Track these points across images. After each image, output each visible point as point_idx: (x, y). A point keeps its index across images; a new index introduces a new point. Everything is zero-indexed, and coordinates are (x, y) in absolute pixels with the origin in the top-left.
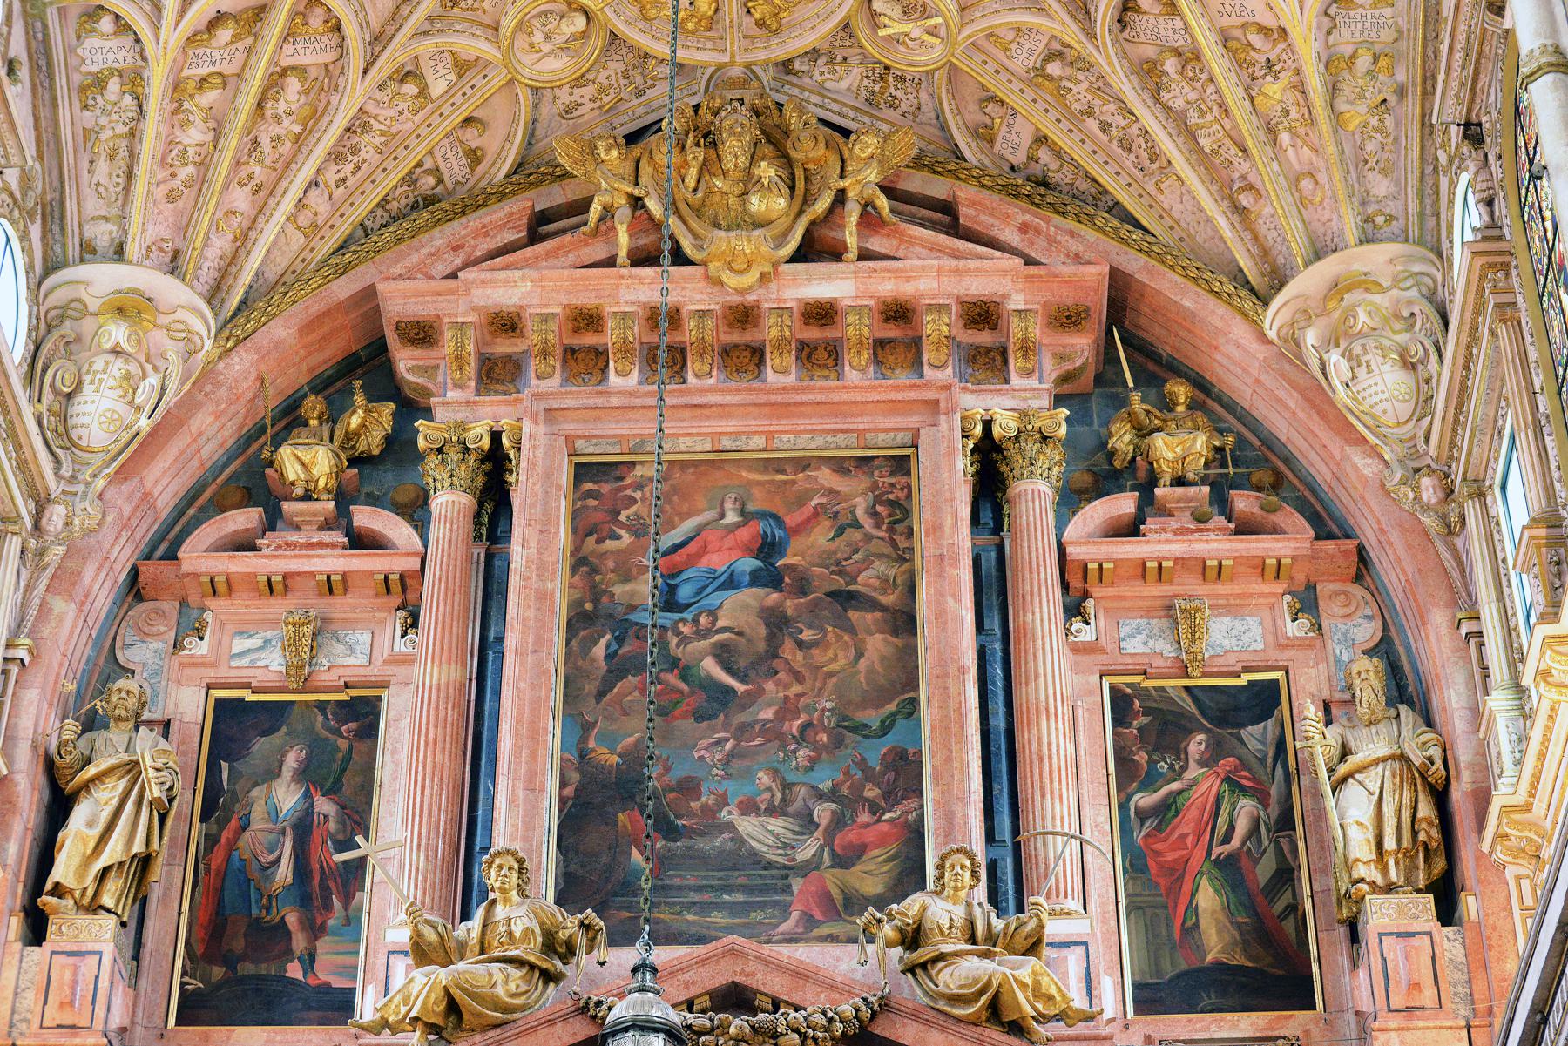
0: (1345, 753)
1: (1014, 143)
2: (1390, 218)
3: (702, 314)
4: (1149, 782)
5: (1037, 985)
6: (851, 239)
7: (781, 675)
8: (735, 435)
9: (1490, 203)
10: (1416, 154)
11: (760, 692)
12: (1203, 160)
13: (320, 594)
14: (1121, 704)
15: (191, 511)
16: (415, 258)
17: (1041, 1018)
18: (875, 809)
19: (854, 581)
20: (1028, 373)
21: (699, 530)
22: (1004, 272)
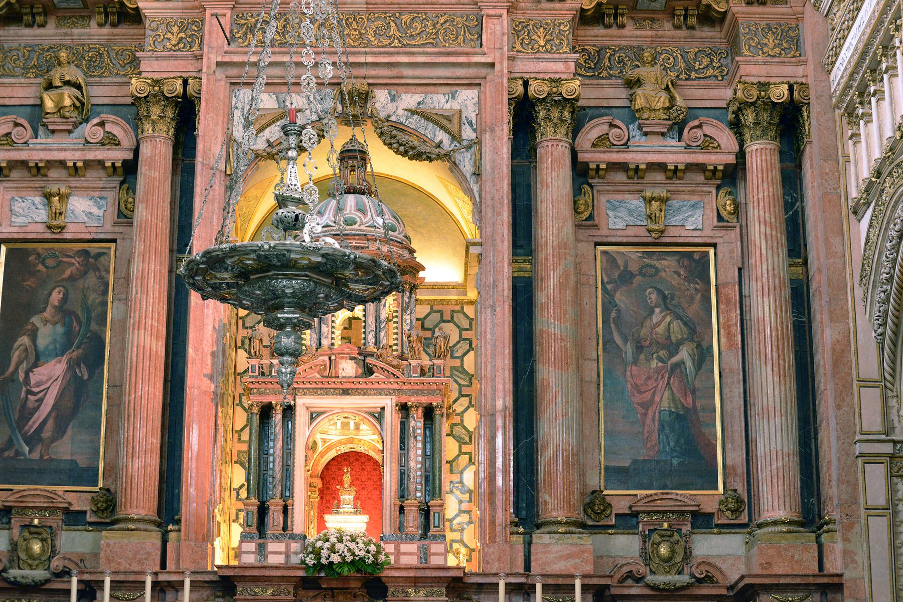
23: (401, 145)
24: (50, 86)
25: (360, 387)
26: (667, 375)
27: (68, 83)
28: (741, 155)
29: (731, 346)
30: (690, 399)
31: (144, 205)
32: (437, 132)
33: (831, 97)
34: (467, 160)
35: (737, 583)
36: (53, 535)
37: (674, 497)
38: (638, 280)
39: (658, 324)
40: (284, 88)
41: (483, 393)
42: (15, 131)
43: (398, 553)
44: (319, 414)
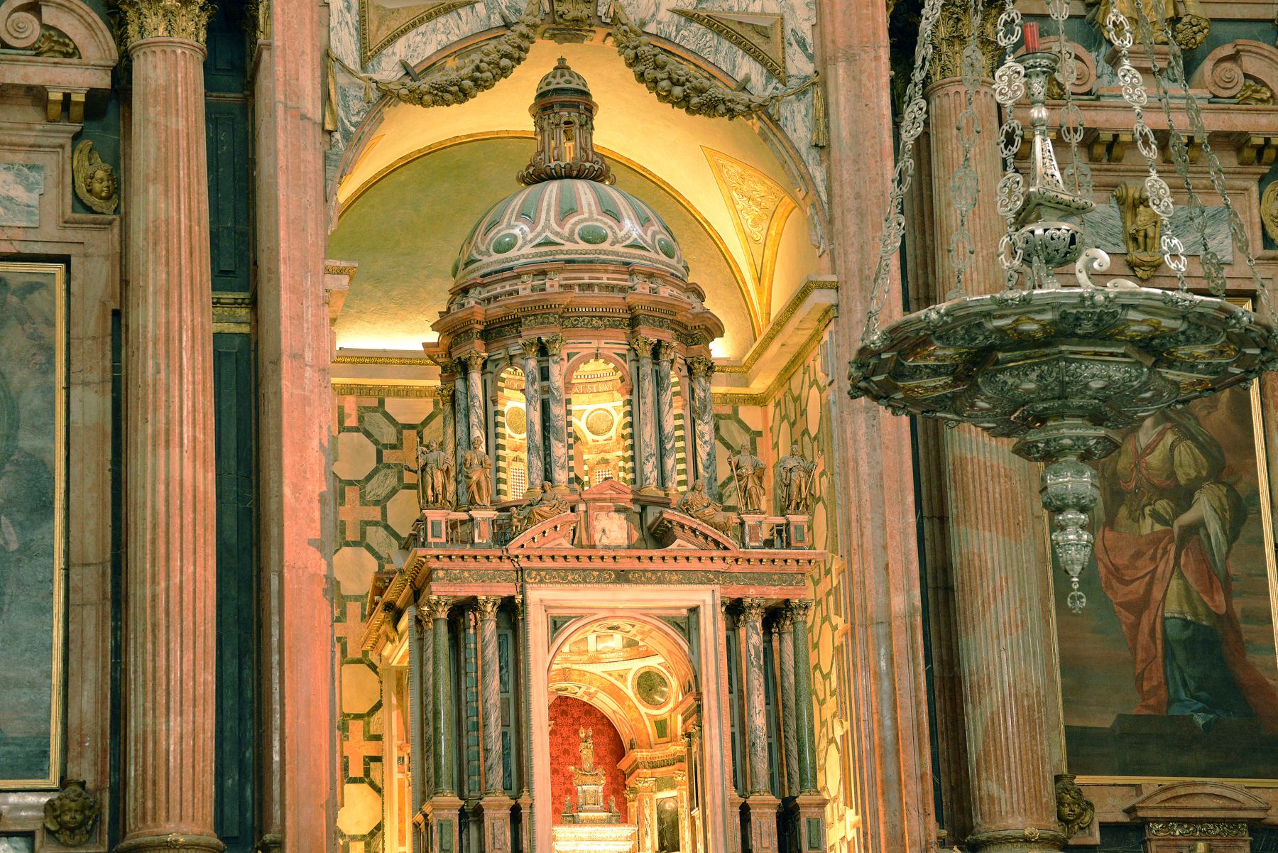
23: (676, 83)
25: (651, 566)
26: (1172, 549)
30: (1220, 598)
31: (161, 188)
32: (739, 60)
34: (799, 118)
37: (1217, 791)
39: (1151, 448)
41: (856, 578)
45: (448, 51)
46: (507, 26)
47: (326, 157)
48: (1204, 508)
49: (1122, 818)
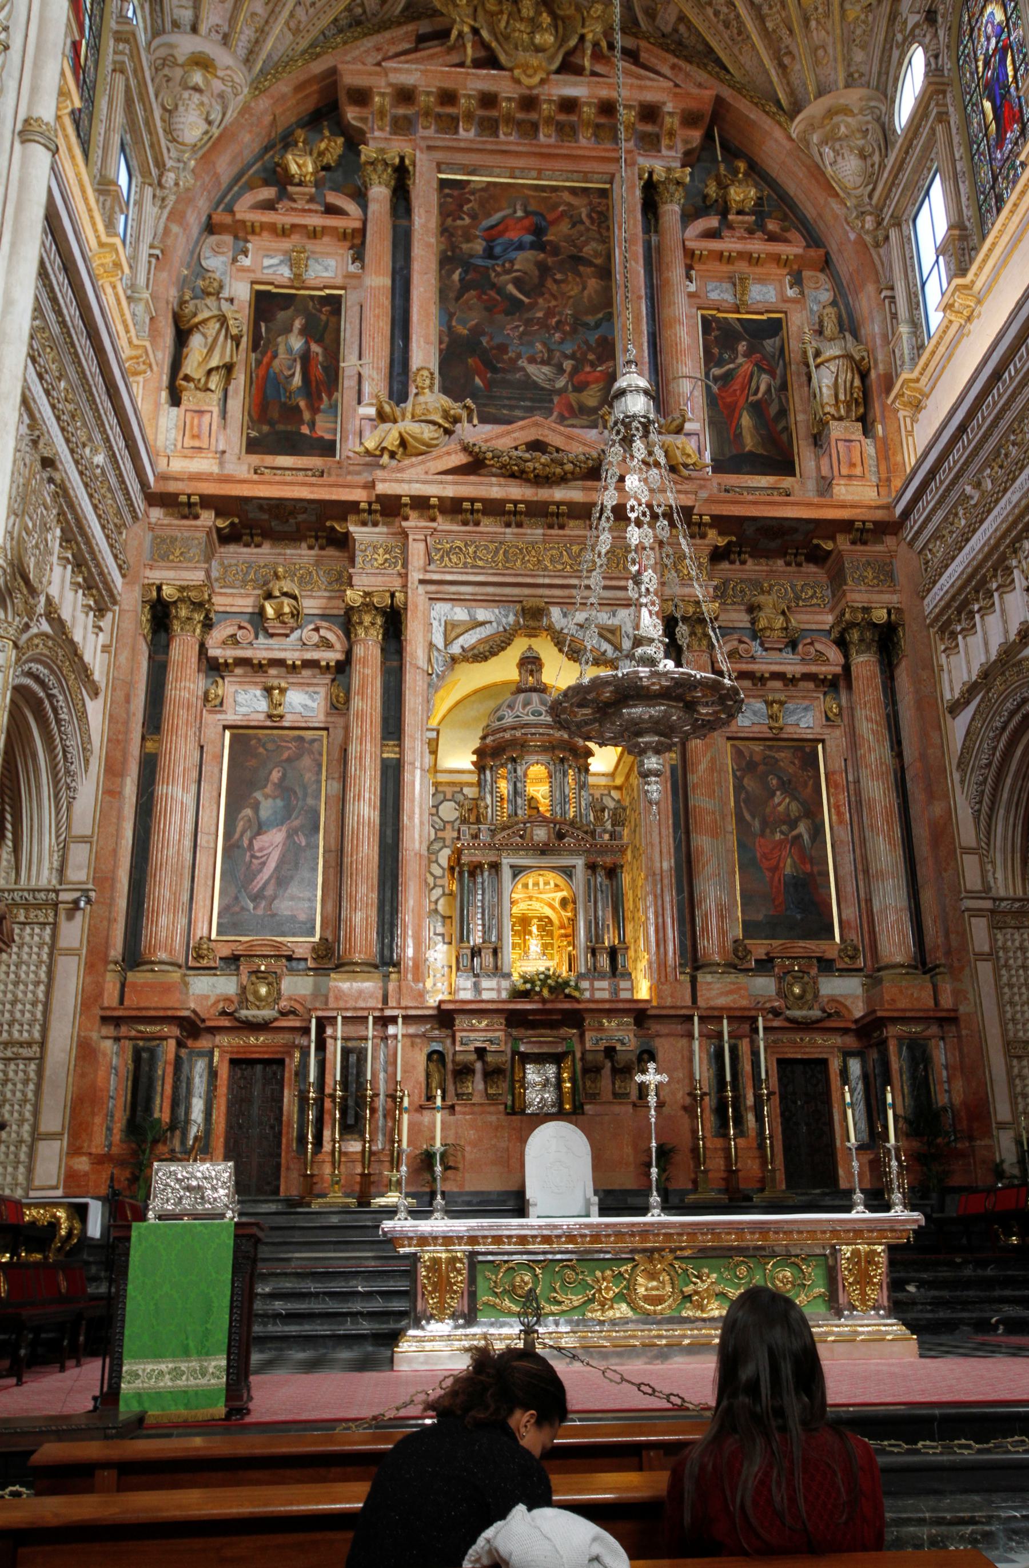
0: (817, 354)
1: (667, 19)
2: (862, 75)
3: (509, 99)
4: (720, 363)
5: (684, 449)
6: (587, 64)
7: (546, 296)
8: (522, 169)
9: (936, 57)
10: (882, 37)
11: (536, 303)
12: (766, 34)
13: (309, 238)
14: (706, 322)
15: (236, 188)
16: (357, 53)
17: (686, 466)
18: (593, 365)
19: (581, 251)
20: (670, 148)
21: (504, 218)
22: (663, 89)
24: (269, 596)
27: (285, 594)
28: (847, 668)
29: (841, 822)
30: (808, 866)
33: (925, 618)
35: (863, 1017)
36: (278, 978)
38: (761, 768)
39: (779, 804)
40: (473, 604)
42: (240, 633)
43: (593, 989)
44: (520, 872)
45: (481, 641)
46: (505, 630)
47: (429, 685)
48: (802, 828)
49: (764, 957)
